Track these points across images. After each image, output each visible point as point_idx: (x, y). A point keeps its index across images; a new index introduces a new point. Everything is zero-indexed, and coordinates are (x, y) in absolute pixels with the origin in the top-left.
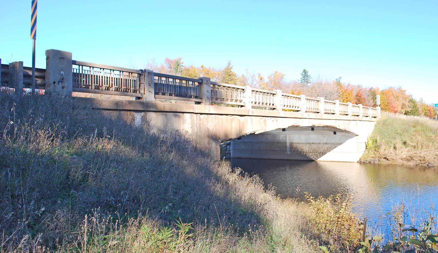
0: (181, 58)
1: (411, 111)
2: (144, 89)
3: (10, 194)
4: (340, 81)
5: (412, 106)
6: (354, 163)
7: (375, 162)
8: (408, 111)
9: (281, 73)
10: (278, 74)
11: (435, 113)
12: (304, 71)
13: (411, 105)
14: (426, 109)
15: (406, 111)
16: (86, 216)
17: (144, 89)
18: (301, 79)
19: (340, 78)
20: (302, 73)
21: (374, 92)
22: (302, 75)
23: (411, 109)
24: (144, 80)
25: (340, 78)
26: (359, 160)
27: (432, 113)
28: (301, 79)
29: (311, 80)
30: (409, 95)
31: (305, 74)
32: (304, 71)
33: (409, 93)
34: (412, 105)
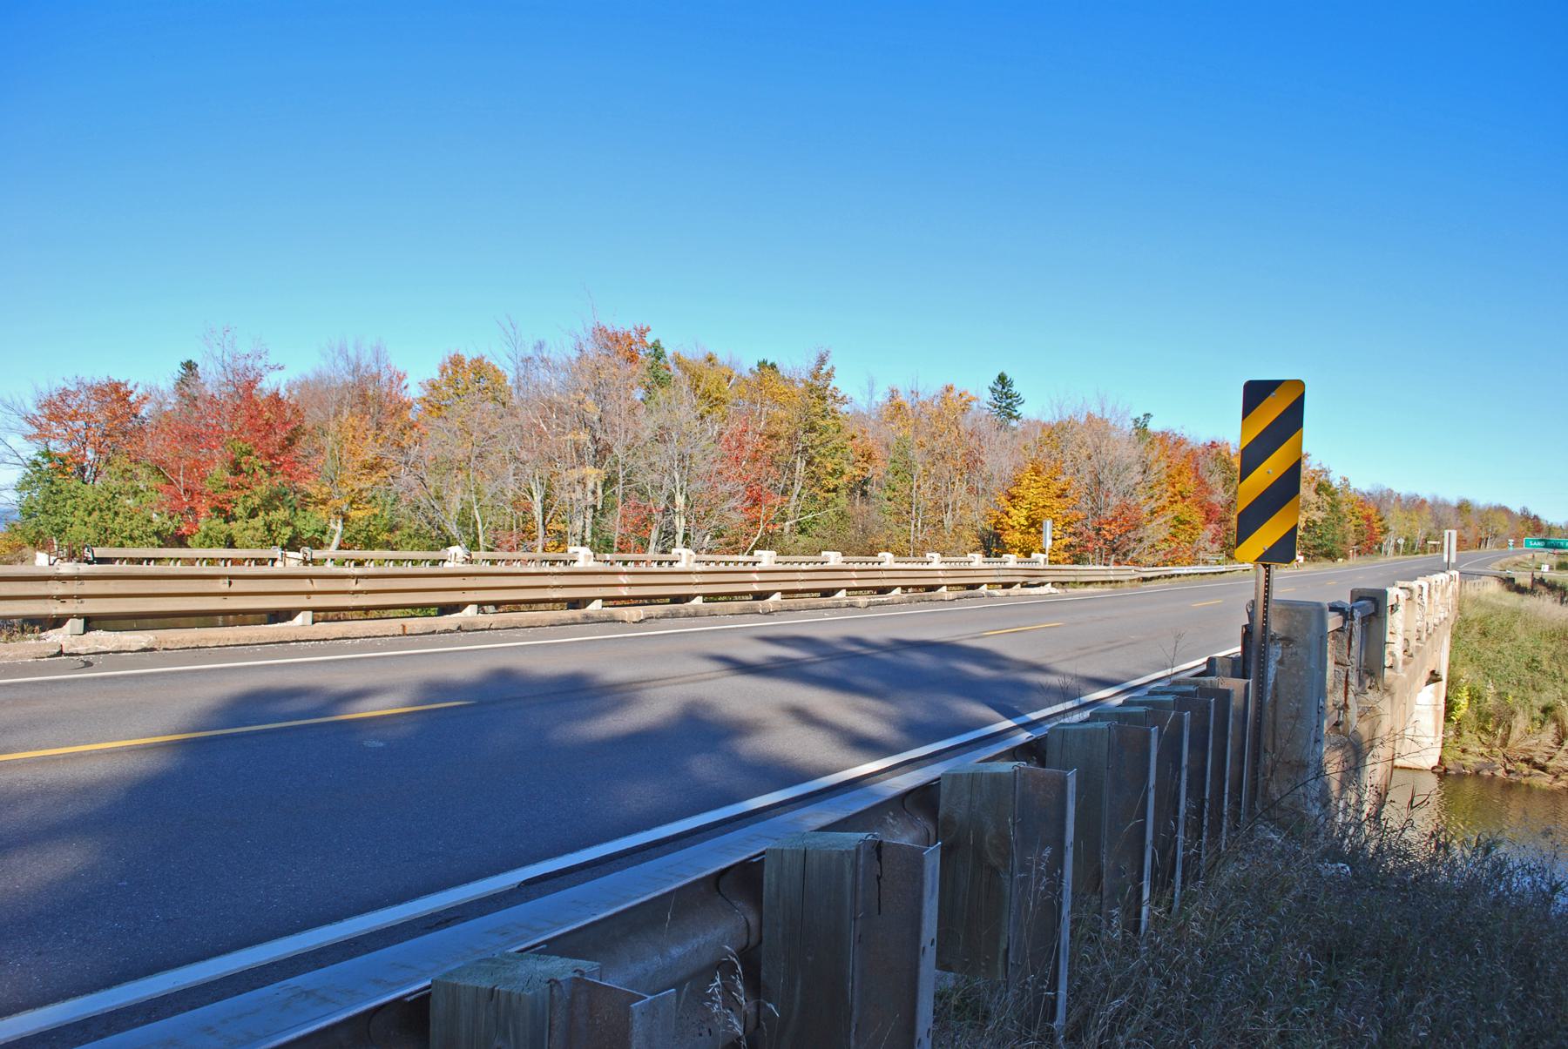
0: (648, 330)
1: (1323, 521)
2: (1346, 688)
3: (636, 1017)
4: (1146, 425)
5: (1327, 508)
6: (1421, 772)
7: (1496, 773)
8: (1314, 522)
9: (966, 392)
10: (955, 394)
11: (1383, 526)
12: (1002, 379)
13: (1325, 504)
14: (1357, 514)
15: (1306, 521)
16: (687, 984)
17: (1346, 688)
18: (990, 404)
19: (1147, 415)
20: (992, 385)
21: (1228, 461)
22: (993, 391)
23: (1322, 515)
24: (1346, 651)
25: (1147, 415)
26: (1436, 764)
27: (1375, 525)
28: (990, 404)
29: (1020, 409)
30: (1318, 469)
31: (1003, 388)
32: (1002, 379)
33: (1320, 464)
34: (1328, 503)
